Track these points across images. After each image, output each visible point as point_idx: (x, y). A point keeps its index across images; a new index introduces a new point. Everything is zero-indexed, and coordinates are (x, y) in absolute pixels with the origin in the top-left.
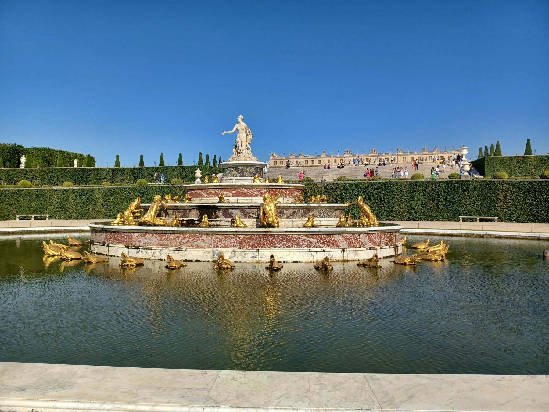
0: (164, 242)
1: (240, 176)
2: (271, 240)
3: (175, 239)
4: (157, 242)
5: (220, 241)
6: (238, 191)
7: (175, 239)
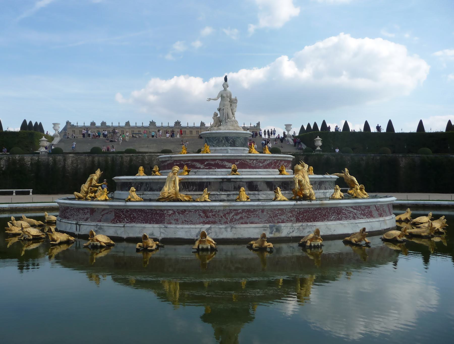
0: (211, 219)
1: (231, 146)
3: (225, 215)
4: (202, 220)
5: (276, 216)
6: (243, 164)
7: (225, 215)
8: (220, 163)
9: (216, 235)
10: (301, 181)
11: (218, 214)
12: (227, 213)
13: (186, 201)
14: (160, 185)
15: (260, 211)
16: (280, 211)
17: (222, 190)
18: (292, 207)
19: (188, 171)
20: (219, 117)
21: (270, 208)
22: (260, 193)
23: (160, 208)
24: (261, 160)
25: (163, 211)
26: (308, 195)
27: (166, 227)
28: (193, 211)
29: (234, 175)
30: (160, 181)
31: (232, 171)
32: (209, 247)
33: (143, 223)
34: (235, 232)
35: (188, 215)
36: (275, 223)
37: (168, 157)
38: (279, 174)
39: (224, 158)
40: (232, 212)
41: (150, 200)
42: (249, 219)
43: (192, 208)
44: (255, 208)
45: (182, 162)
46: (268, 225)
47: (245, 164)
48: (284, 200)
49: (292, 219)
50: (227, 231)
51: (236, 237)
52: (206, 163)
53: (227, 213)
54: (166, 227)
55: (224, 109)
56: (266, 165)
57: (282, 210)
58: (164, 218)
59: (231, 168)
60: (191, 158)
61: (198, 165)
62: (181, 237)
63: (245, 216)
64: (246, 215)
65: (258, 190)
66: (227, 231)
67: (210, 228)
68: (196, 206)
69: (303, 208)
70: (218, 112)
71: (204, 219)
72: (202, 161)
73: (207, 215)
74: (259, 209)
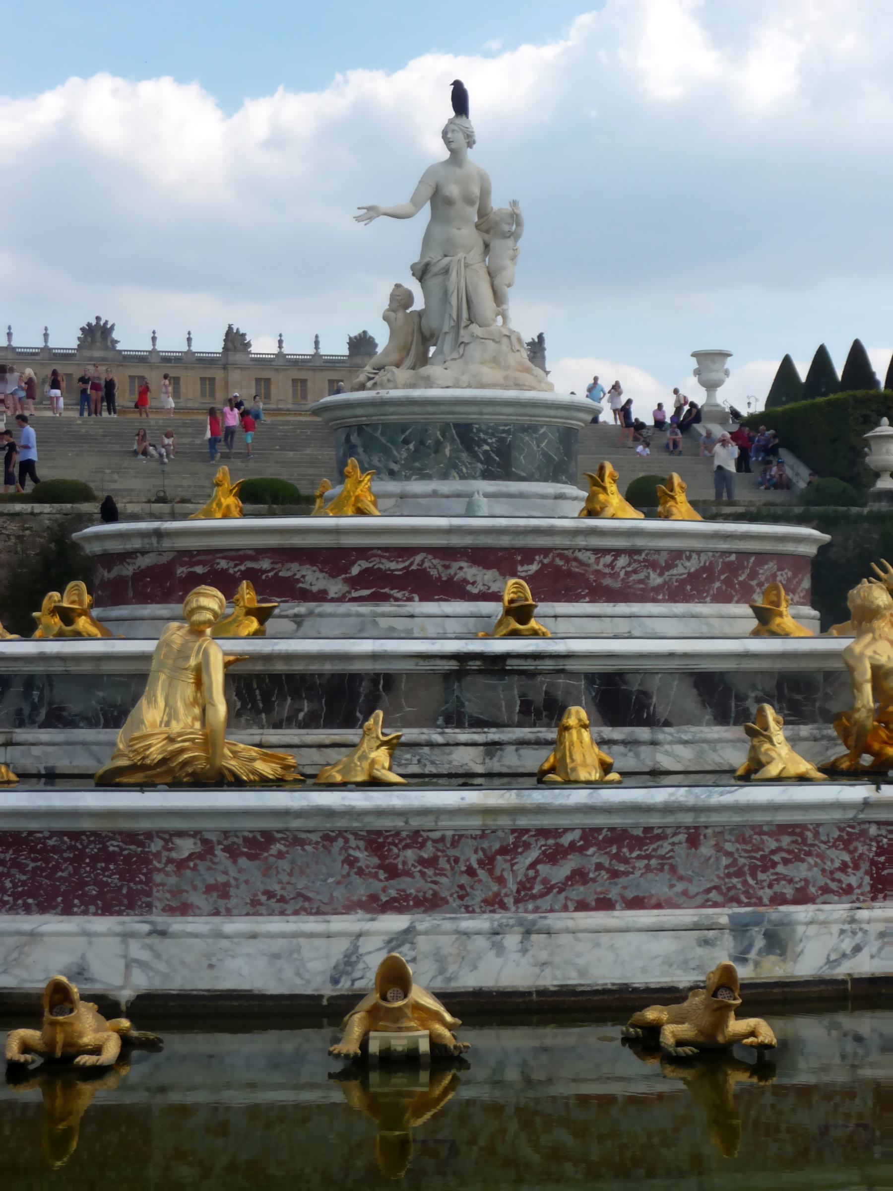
0: (412, 885)
1: (487, 475)
3: (488, 862)
4: (362, 889)
5: (767, 864)
7: (488, 862)
8: (434, 567)
9: (441, 971)
11: (452, 852)
12: (503, 851)
13: (264, 783)
14: (114, 694)
15: (682, 837)
16: (786, 840)
17: (455, 718)
18: (850, 814)
19: (263, 615)
20: (420, 314)
21: (737, 819)
22: (660, 736)
23: (126, 825)
24: (658, 551)
25: (140, 844)
27: (163, 934)
28: (315, 837)
29: (514, 634)
30: (108, 668)
31: (508, 612)
32: (424, 1046)
33: (28, 910)
34: (543, 956)
35: (284, 864)
36: (760, 902)
37: (142, 534)
38: (756, 634)
39: (455, 541)
40: (527, 846)
41: (51, 778)
42: (622, 881)
43: (311, 824)
44: (654, 820)
45: (223, 564)
46: (722, 915)
47: (570, 574)
48: (803, 779)
49: (853, 880)
50: (500, 949)
51: (550, 980)
52: (355, 570)
53: (503, 851)
54: (163, 934)
55: (446, 271)
56: (682, 582)
57: (796, 834)
58: (149, 881)
59: (496, 597)
60: (274, 541)
61: (313, 578)
62: (245, 985)
63: (599, 867)
64: (605, 861)
65: (651, 722)
66: (500, 949)
67: (408, 935)
68: (330, 813)
70: (414, 286)
71: (376, 886)
72: (333, 558)
73: (390, 864)
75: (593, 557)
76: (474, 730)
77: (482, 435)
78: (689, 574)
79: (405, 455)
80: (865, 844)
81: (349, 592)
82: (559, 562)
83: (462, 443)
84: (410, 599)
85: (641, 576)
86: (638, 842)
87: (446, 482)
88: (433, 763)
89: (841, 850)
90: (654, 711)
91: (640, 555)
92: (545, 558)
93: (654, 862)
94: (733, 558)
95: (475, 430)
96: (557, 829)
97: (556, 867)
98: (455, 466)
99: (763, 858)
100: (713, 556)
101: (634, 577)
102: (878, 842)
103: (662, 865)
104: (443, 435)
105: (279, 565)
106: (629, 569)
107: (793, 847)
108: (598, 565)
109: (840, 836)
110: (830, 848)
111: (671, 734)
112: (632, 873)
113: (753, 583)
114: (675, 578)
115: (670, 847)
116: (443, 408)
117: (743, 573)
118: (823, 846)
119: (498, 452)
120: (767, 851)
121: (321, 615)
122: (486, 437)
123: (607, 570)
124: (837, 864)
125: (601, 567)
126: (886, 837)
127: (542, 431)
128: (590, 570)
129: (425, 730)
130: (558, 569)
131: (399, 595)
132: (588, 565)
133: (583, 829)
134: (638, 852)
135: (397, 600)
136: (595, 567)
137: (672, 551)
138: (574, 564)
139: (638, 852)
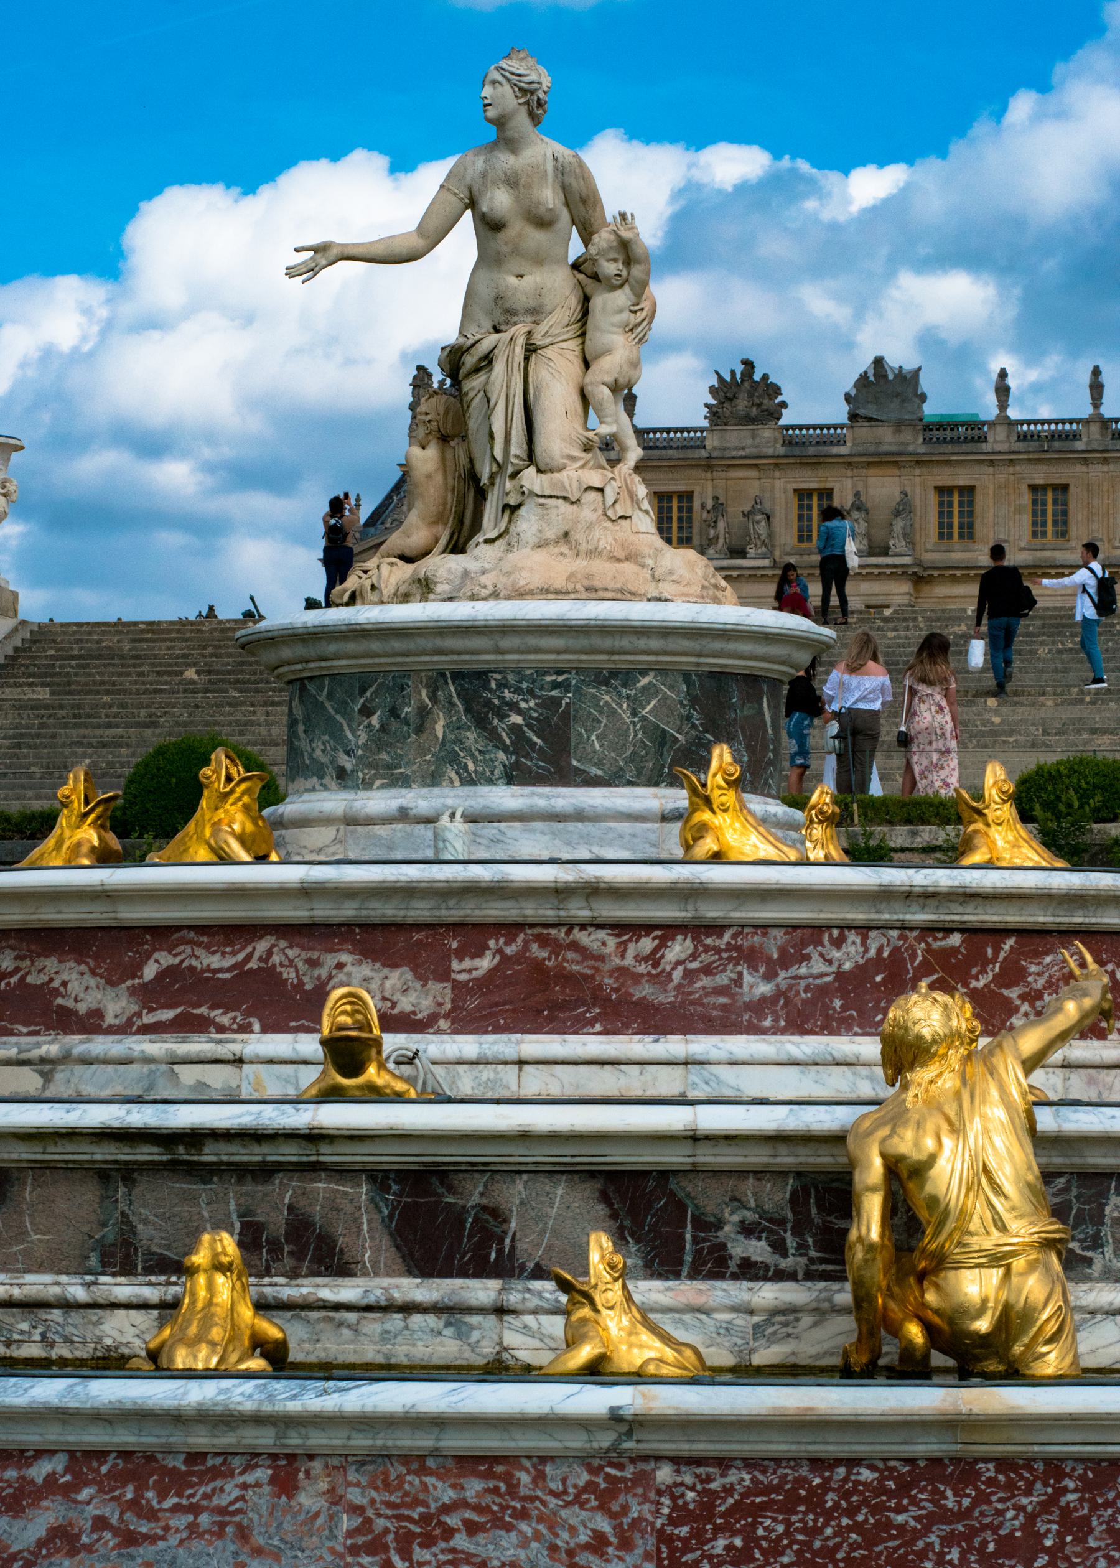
1: (514, 776)
2: (1012, 1522)
6: (536, 969)
10: (920, 1170)
15: (262, 1474)
16: (474, 1487)
18: (605, 1440)
24: (763, 927)
26: (983, 1325)
39: (323, 911)
44: (201, 1440)
52: (150, 971)
55: (488, 360)
56: (823, 992)
61: (79, 985)
63: (101, 1523)
65: (506, 1268)
69: (750, 1463)
74: (253, 1458)
75: (612, 942)
76: (153, 1278)
77: (507, 694)
78: (839, 975)
79: (363, 738)
80: (645, 1499)
81: (139, 1015)
82: (537, 952)
83: (468, 710)
84: (246, 1029)
85: (723, 979)
86: (176, 1482)
87: (436, 791)
88: (68, 1341)
89: (592, 1509)
90: (513, 1248)
91: (720, 936)
92: (507, 944)
93: (204, 1519)
94: (955, 939)
95: (493, 685)
96: (22, 1451)
97: (19, 1524)
98: (453, 759)
99: (426, 1519)
100: (902, 937)
101: (705, 981)
102: (674, 1498)
103: (222, 1525)
104: (434, 699)
105: (28, 962)
106: (694, 965)
107: (488, 1499)
108: (623, 957)
109: (589, 1484)
110: (568, 1504)
111: (539, 1294)
112: (163, 1538)
113: (1013, 993)
114: (803, 983)
115: (237, 1493)
116: (423, 643)
117: (983, 971)
118: (553, 1502)
119: (541, 726)
120: (433, 1506)
121: (87, 1061)
122: (516, 698)
123: (642, 968)
124: (583, 1538)
125: (629, 961)
126: (692, 1489)
127: (644, 681)
128: (606, 967)
129: (64, 1278)
130: (538, 966)
131: (225, 1020)
132: (601, 958)
133: (72, 1453)
134: (175, 1500)
135: (221, 1029)
136: (617, 961)
137: (795, 927)
138: (570, 955)
139: (175, 1500)
